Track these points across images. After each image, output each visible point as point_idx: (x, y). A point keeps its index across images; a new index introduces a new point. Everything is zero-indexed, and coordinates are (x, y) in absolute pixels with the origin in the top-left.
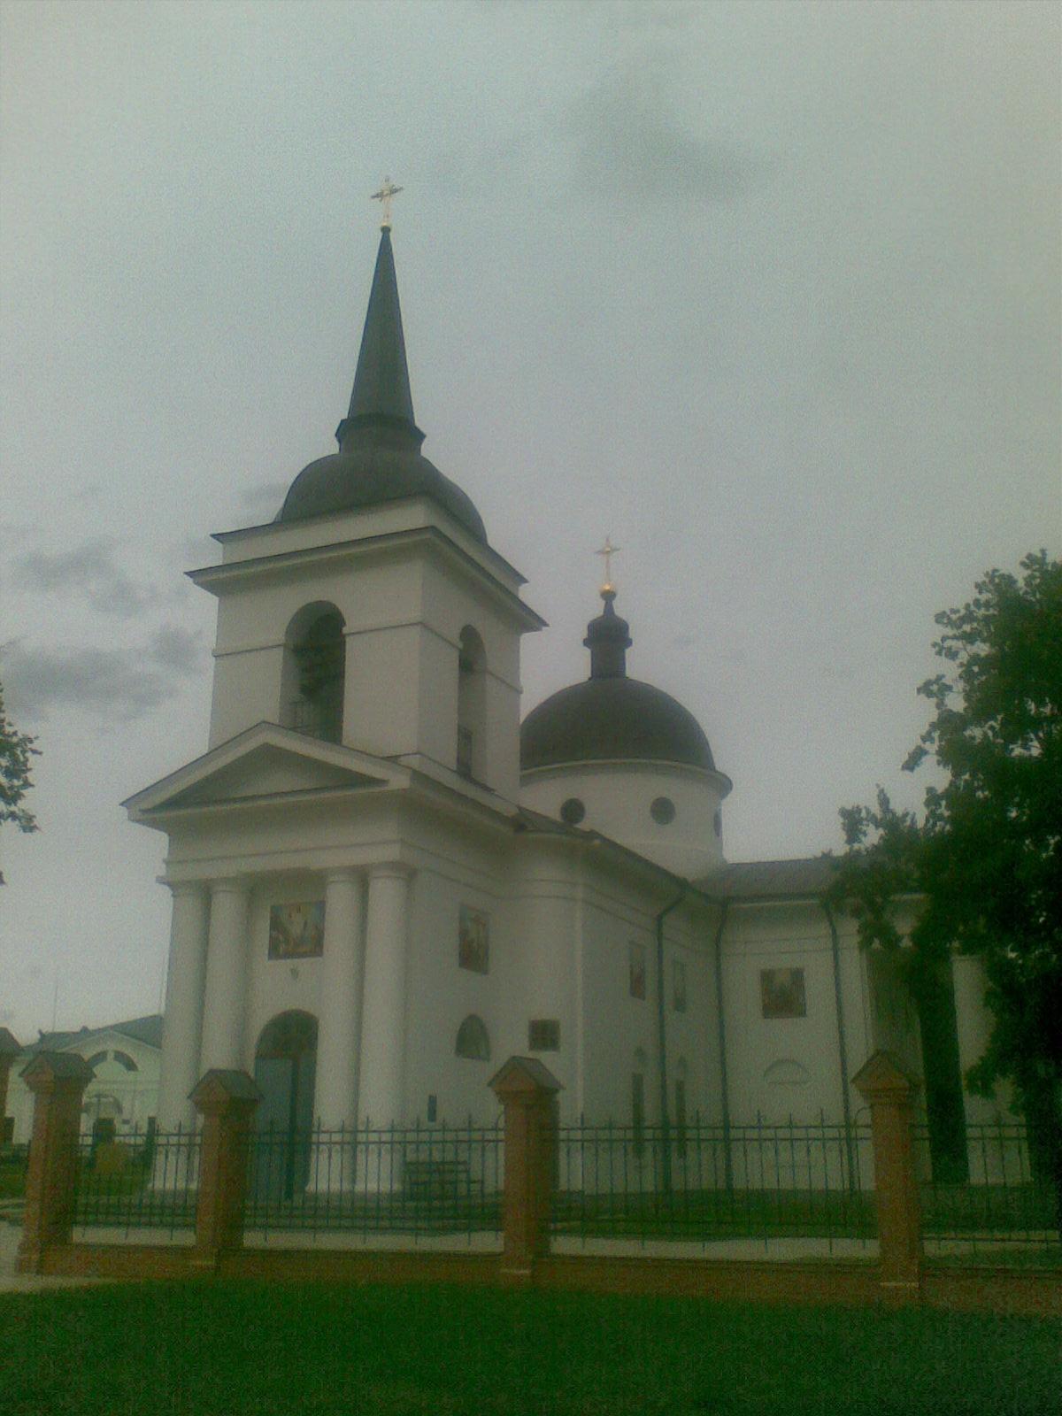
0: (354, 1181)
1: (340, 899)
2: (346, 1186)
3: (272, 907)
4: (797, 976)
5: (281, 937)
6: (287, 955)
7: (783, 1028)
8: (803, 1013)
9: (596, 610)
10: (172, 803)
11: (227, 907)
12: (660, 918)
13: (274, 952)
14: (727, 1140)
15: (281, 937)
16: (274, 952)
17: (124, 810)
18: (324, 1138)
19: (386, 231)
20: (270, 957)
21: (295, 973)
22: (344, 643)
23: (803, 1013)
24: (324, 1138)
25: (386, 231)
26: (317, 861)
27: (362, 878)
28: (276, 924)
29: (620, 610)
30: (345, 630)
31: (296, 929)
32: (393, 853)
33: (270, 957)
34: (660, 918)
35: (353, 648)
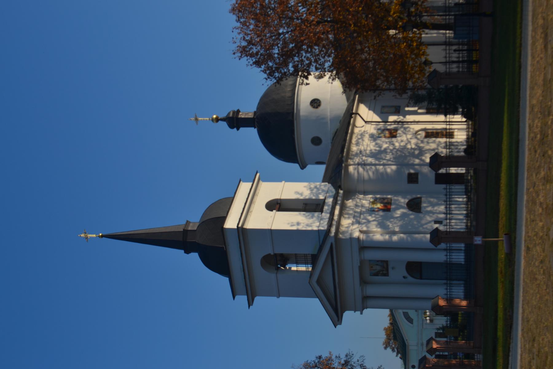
0: (461, 250)
2: (463, 252)
3: (371, 275)
6: (387, 270)
9: (224, 124)
10: (336, 310)
11: (371, 290)
12: (366, 122)
13: (387, 274)
14: (450, 250)
16: (387, 274)
17: (338, 326)
18: (448, 260)
20: (388, 276)
21: (393, 268)
24: (448, 260)
26: (357, 264)
28: (376, 274)
29: (223, 115)
30: (272, 254)
31: (378, 268)
33: (388, 276)
34: (366, 122)
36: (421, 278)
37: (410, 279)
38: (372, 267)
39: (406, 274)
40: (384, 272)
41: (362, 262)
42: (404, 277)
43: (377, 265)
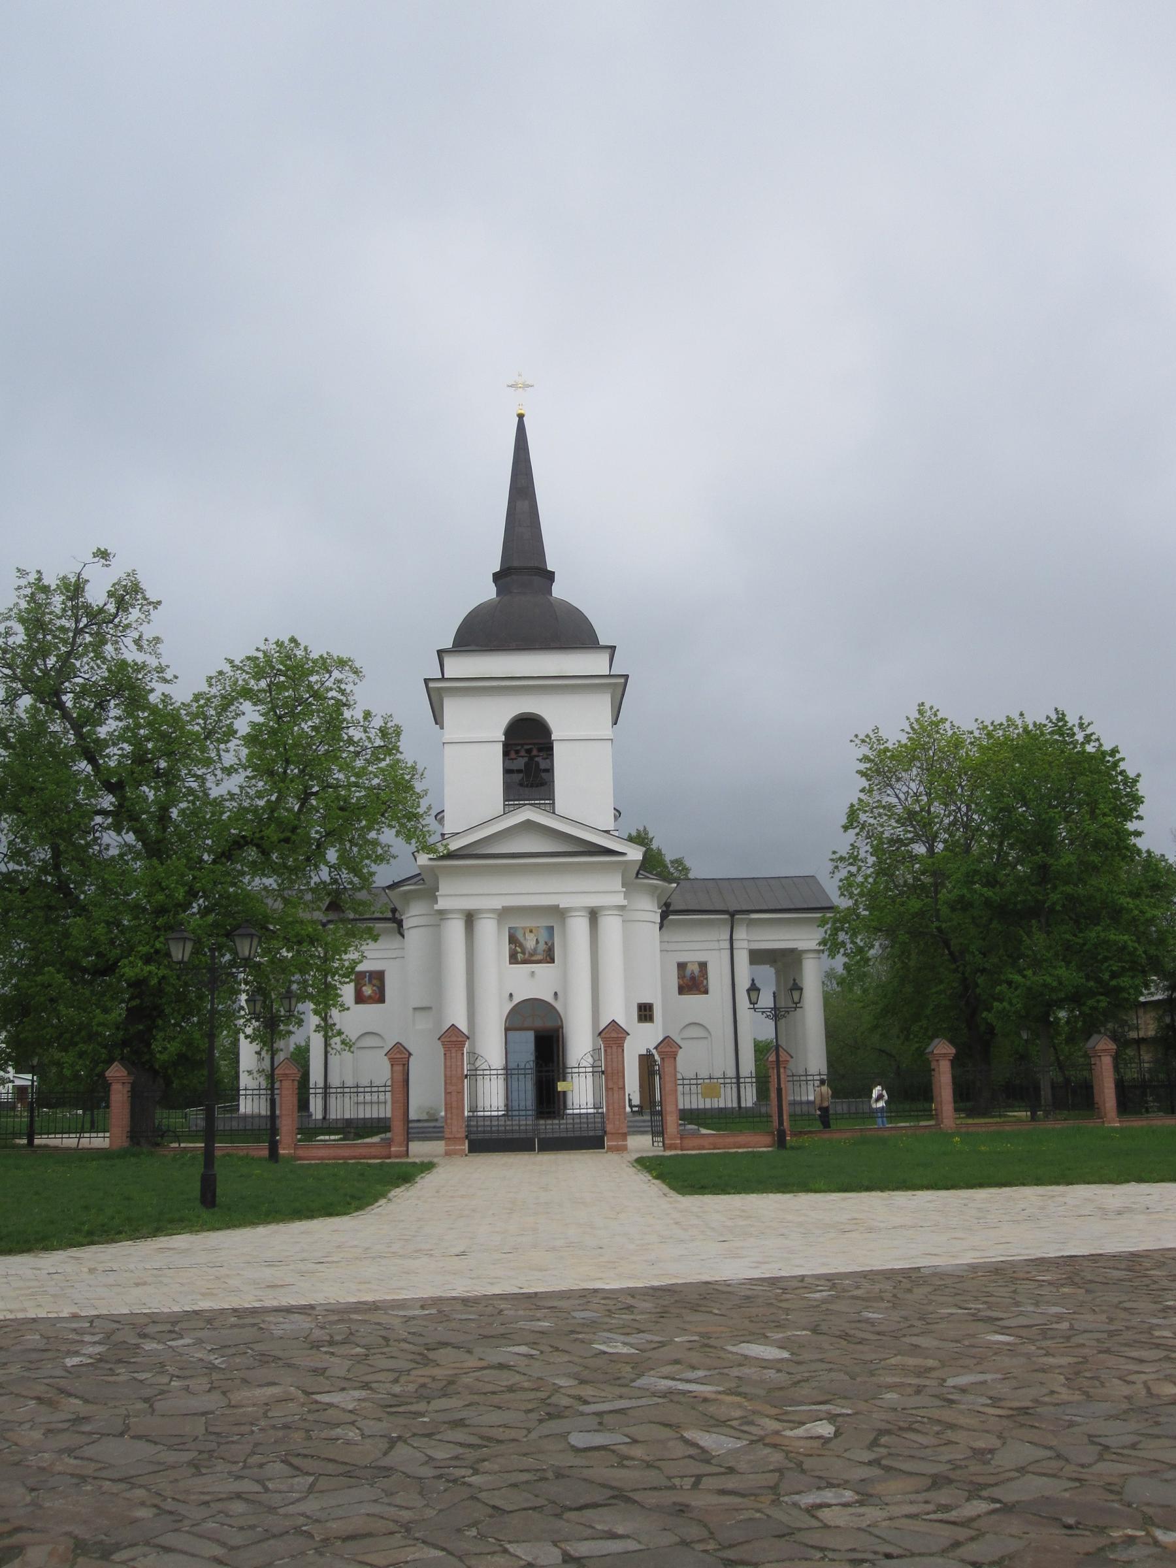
1: (579, 926)
4: (703, 966)
5: (519, 950)
6: (524, 962)
7: (693, 1000)
8: (706, 992)
13: (513, 959)
15: (519, 950)
16: (513, 959)
19: (521, 417)
22: (552, 749)
23: (706, 992)
25: (521, 417)
27: (594, 915)
28: (513, 939)
31: (530, 944)
32: (620, 900)
35: (560, 752)
36: (507, 1030)
37: (509, 1007)
38: (531, 931)
39: (516, 1000)
40: (520, 956)
41: (559, 913)
42: (511, 995)
43: (537, 942)
